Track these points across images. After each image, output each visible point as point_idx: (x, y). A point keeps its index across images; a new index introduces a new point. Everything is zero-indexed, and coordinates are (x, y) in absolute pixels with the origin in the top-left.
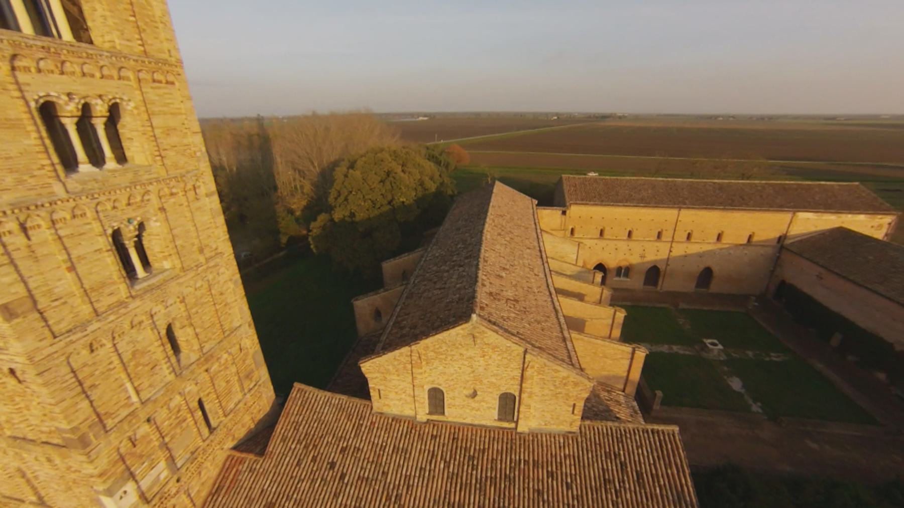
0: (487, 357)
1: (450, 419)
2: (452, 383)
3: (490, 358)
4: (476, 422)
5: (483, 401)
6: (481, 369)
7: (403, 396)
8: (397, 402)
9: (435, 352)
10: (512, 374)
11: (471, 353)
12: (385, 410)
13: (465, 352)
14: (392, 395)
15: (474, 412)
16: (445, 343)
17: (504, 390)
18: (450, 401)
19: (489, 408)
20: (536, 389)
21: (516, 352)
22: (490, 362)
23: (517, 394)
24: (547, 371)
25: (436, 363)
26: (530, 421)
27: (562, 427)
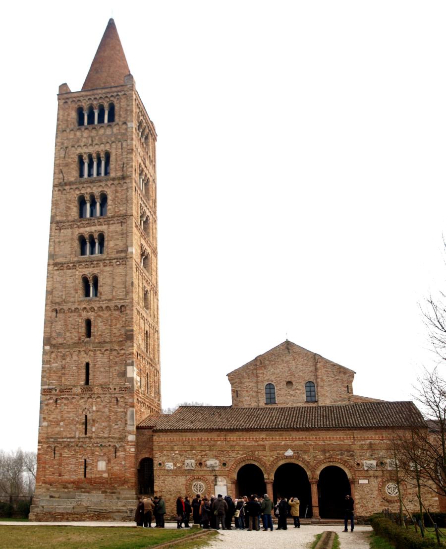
1: (279, 406)
4: (295, 405)
5: (297, 389)
6: (294, 368)
7: (251, 393)
9: (269, 361)
11: (288, 358)
13: (284, 359)
14: (244, 393)
15: (292, 397)
16: (274, 355)
17: (307, 379)
18: (279, 392)
19: (300, 393)
20: (325, 378)
22: (298, 363)
23: (314, 381)
24: (328, 366)
27: (344, 402)
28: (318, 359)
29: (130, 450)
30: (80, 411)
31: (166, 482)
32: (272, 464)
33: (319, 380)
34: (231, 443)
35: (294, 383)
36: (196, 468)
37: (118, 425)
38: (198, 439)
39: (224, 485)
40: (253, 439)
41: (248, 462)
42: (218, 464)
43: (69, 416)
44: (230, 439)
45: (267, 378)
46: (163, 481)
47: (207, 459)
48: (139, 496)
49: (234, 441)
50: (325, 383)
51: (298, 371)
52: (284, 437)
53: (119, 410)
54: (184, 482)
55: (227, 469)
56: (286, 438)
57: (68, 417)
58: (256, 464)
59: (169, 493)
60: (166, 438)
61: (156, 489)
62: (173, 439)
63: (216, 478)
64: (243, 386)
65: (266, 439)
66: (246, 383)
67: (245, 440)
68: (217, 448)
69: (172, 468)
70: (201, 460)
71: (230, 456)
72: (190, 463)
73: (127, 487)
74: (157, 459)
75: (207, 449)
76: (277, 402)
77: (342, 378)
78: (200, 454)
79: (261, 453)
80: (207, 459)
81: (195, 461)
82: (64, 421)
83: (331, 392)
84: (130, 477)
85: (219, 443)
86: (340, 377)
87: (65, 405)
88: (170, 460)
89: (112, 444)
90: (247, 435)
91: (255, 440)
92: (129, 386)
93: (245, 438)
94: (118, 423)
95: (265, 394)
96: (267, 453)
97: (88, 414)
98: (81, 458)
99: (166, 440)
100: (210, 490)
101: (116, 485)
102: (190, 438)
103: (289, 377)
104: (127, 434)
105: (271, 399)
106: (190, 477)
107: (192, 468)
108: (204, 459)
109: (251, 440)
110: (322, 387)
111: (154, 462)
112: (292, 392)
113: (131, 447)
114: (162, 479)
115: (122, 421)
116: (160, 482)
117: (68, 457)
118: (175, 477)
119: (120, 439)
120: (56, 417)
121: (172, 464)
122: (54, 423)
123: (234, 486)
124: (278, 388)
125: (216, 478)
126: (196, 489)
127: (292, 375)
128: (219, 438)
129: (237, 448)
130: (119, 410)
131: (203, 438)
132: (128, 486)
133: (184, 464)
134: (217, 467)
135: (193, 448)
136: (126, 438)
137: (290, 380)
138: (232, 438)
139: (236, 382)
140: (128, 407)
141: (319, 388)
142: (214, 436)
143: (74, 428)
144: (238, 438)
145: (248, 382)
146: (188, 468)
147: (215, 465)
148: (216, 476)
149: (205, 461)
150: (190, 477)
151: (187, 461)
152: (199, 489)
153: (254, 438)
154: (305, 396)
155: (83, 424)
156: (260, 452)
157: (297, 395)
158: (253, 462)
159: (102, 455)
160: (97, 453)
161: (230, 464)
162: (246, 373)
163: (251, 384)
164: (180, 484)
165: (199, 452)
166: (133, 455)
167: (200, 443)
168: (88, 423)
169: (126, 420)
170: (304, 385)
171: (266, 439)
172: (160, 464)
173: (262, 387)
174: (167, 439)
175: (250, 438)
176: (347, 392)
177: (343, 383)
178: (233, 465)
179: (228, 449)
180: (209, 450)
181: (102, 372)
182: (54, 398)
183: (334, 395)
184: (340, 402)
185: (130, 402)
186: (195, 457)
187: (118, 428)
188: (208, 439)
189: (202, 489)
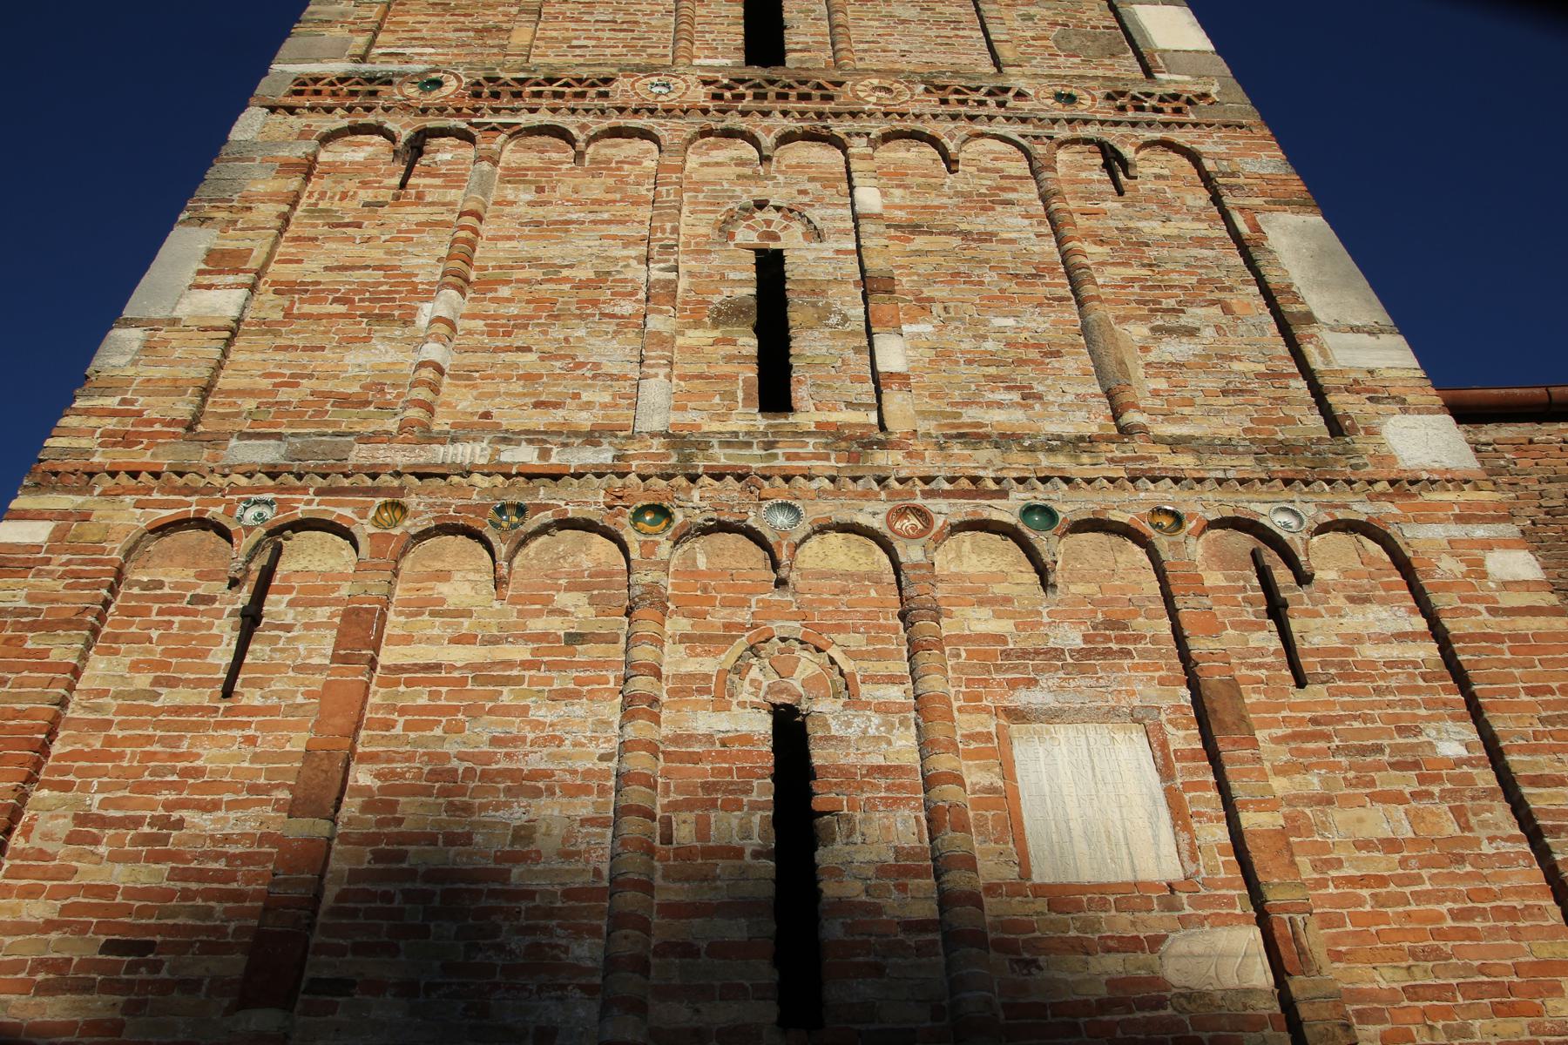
29: (1477, 569)
30: (695, 224)
37: (1191, 332)
43: (551, 251)
57: (534, 262)
82: (461, 283)
87: (515, 176)
89: (1202, 505)
92: (1199, 89)
97: (792, 241)
98: (719, 692)
117: (482, 673)
120: (376, 255)
122: (341, 309)
140: (1259, 201)
143: (614, 353)
155: (727, 314)
159: (1071, 637)
160: (981, 621)
168: (795, 317)
181: (903, 22)
182: (403, 126)
187: (1205, 363)
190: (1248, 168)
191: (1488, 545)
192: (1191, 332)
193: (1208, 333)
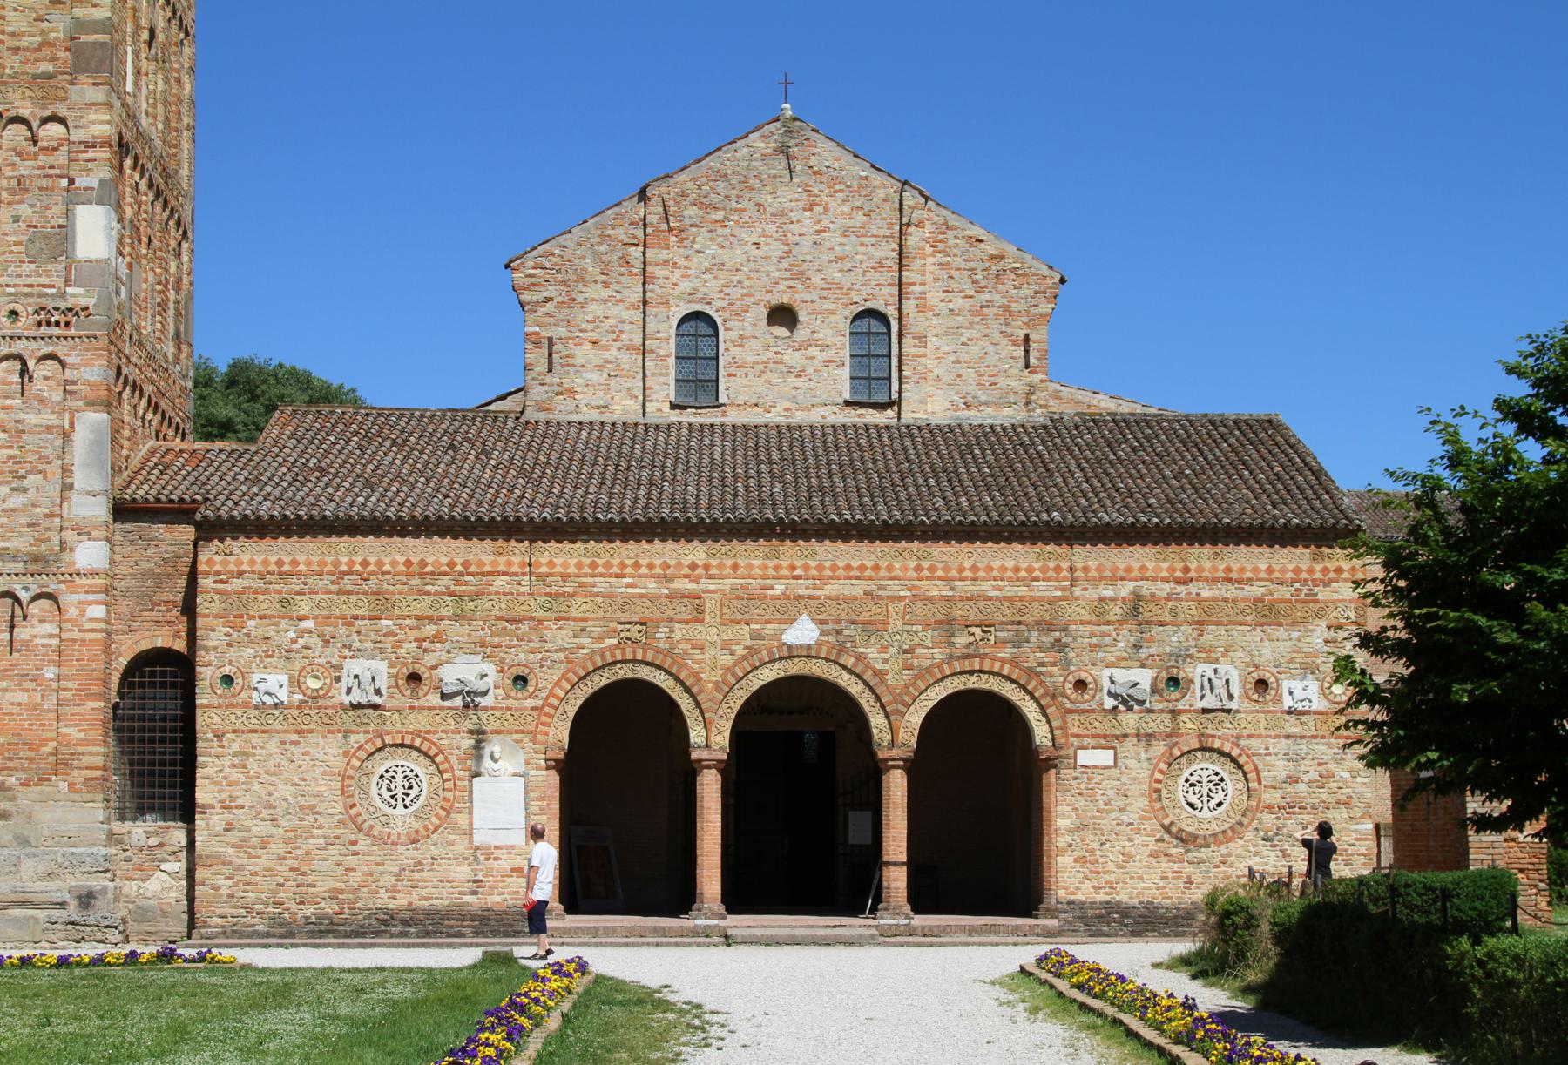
0: (818, 209)
1: (734, 417)
2: (736, 293)
3: (826, 209)
4: (798, 418)
5: (809, 343)
6: (806, 243)
8: (594, 376)
10: (877, 254)
12: (563, 410)
14: (583, 354)
15: (792, 379)
18: (735, 351)
19: (828, 362)
20: (934, 297)
21: (881, 193)
22: (825, 223)
23: (891, 312)
25: (702, 236)
26: (929, 402)
27: (1007, 411)
28: (913, 208)
29: (82, 613)
31: (251, 761)
32: (725, 682)
33: (909, 306)
34: (556, 585)
35: (802, 316)
36: (391, 696)
37: (25, 490)
38: (408, 563)
39: (516, 775)
40: (651, 566)
41: (623, 672)
42: (490, 680)
44: (551, 564)
45: (686, 286)
46: (236, 760)
47: (444, 656)
48: (118, 827)
49: (565, 577)
50: (935, 321)
51: (825, 258)
52: (785, 563)
53: (32, 419)
54: (338, 762)
55: (529, 703)
56: (793, 568)
58: (661, 680)
59: (265, 813)
60: (259, 559)
61: (203, 794)
62: (295, 563)
63: (478, 747)
64: (581, 318)
65: (707, 567)
66: (595, 309)
67: (615, 570)
68: (488, 605)
69: (283, 695)
70: (417, 661)
71: (548, 646)
72: (371, 672)
73: (64, 786)
74: (212, 657)
75: (444, 612)
76: (722, 399)
77: (1005, 301)
78: (414, 634)
79: (680, 632)
80: (444, 656)
81: (391, 665)
83: (958, 362)
84: (82, 742)
85: (500, 582)
86: (997, 297)
88: (274, 661)
90: (626, 552)
91: (658, 571)
93: (616, 561)
94: (25, 483)
95: (672, 361)
96: (709, 632)
99: (258, 568)
100: (450, 795)
101: (11, 781)
102: (372, 560)
103: (782, 287)
104: (69, 536)
105: (699, 382)
106: (361, 738)
107: (377, 700)
108: (430, 659)
109: (644, 570)
110: (922, 339)
111: (198, 669)
112: (792, 358)
113: (91, 597)
114: (235, 747)
115: (44, 473)
116: (227, 761)
118: (295, 737)
119: (36, 559)
121: (284, 679)
123: (554, 778)
124: (734, 334)
125: (479, 741)
126: (386, 795)
127: (799, 275)
128: (502, 559)
129: (578, 608)
130: (32, 419)
131: (430, 560)
132: (71, 785)
133: (338, 679)
134: (486, 693)
135: (382, 604)
136: (66, 557)
137: (786, 301)
138: (558, 561)
139: (549, 299)
140: (80, 403)
141: (907, 341)
142: (481, 552)
144: (587, 561)
145: (605, 301)
146: (356, 697)
147: (481, 686)
148: (480, 736)
149: (435, 667)
150: (361, 738)
151: (354, 666)
152: (400, 791)
153: (658, 562)
154: (845, 373)
156: (677, 626)
157: (810, 371)
158: (645, 673)
161: (547, 679)
162: (596, 255)
163: (615, 310)
164: (319, 770)
165: (408, 622)
166: (100, 636)
167: (416, 581)
169: (66, 471)
170: (845, 327)
171: (707, 567)
172: (228, 680)
173: (665, 326)
174: (265, 562)
175: (637, 565)
176: (1022, 362)
177: (1007, 324)
178: (557, 684)
179: (540, 614)
180: (455, 618)
183: (969, 374)
184: (989, 410)
185: (88, 384)
186: (388, 644)
188: (452, 564)
189: (413, 793)
190: (86, 376)
191: (90, 603)
192: (25, 490)
193: (32, 491)
